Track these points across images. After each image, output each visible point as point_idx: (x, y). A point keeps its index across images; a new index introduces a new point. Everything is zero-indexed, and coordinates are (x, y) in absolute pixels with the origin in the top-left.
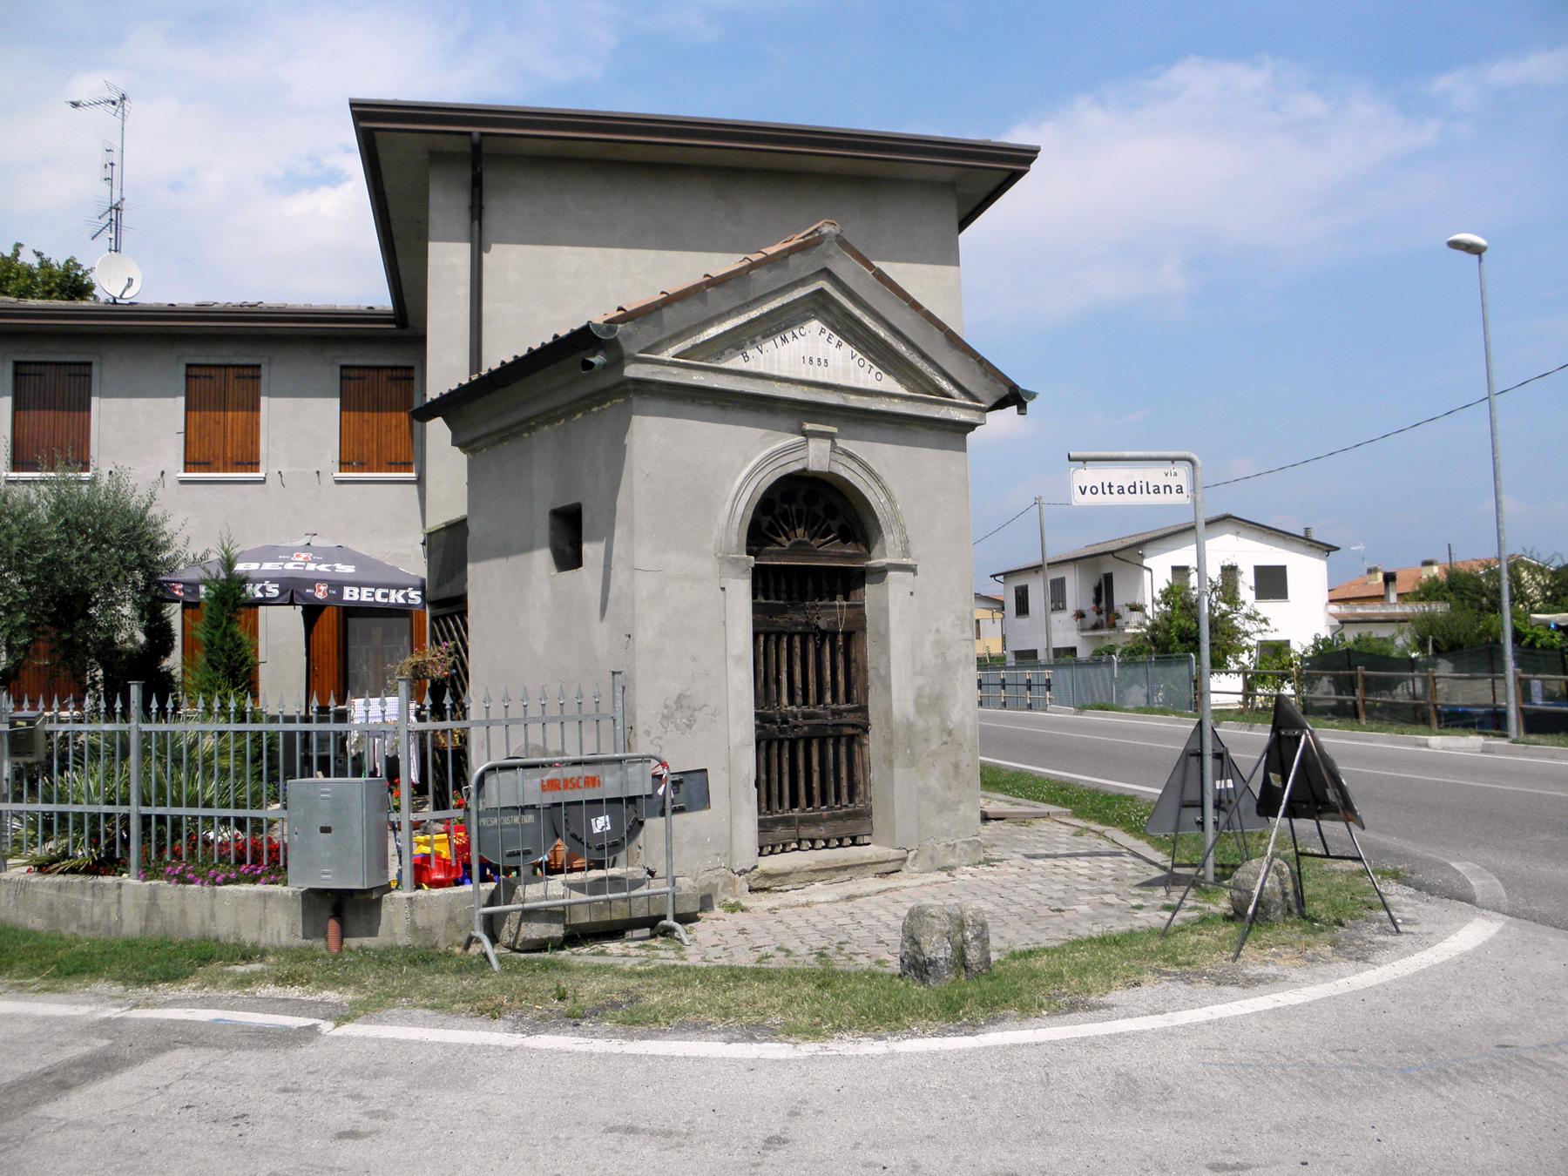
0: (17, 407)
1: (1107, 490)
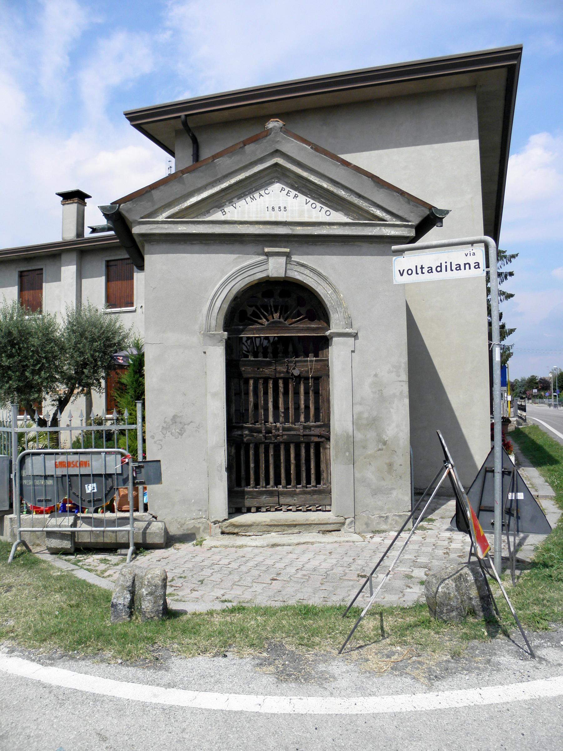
0: (108, 281)
1: (419, 271)
